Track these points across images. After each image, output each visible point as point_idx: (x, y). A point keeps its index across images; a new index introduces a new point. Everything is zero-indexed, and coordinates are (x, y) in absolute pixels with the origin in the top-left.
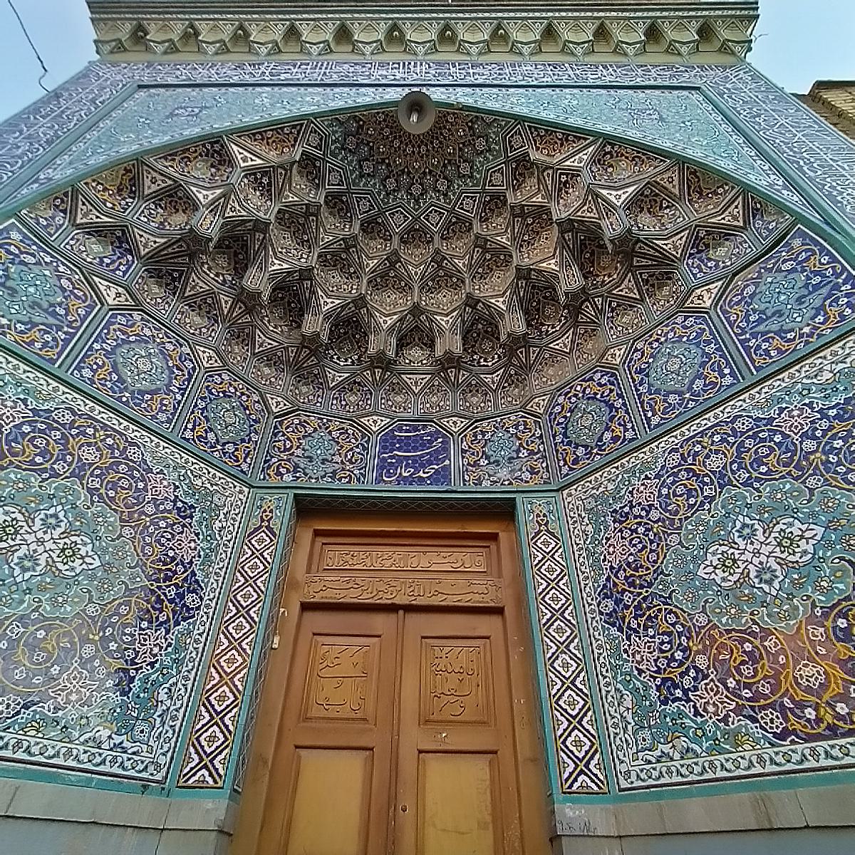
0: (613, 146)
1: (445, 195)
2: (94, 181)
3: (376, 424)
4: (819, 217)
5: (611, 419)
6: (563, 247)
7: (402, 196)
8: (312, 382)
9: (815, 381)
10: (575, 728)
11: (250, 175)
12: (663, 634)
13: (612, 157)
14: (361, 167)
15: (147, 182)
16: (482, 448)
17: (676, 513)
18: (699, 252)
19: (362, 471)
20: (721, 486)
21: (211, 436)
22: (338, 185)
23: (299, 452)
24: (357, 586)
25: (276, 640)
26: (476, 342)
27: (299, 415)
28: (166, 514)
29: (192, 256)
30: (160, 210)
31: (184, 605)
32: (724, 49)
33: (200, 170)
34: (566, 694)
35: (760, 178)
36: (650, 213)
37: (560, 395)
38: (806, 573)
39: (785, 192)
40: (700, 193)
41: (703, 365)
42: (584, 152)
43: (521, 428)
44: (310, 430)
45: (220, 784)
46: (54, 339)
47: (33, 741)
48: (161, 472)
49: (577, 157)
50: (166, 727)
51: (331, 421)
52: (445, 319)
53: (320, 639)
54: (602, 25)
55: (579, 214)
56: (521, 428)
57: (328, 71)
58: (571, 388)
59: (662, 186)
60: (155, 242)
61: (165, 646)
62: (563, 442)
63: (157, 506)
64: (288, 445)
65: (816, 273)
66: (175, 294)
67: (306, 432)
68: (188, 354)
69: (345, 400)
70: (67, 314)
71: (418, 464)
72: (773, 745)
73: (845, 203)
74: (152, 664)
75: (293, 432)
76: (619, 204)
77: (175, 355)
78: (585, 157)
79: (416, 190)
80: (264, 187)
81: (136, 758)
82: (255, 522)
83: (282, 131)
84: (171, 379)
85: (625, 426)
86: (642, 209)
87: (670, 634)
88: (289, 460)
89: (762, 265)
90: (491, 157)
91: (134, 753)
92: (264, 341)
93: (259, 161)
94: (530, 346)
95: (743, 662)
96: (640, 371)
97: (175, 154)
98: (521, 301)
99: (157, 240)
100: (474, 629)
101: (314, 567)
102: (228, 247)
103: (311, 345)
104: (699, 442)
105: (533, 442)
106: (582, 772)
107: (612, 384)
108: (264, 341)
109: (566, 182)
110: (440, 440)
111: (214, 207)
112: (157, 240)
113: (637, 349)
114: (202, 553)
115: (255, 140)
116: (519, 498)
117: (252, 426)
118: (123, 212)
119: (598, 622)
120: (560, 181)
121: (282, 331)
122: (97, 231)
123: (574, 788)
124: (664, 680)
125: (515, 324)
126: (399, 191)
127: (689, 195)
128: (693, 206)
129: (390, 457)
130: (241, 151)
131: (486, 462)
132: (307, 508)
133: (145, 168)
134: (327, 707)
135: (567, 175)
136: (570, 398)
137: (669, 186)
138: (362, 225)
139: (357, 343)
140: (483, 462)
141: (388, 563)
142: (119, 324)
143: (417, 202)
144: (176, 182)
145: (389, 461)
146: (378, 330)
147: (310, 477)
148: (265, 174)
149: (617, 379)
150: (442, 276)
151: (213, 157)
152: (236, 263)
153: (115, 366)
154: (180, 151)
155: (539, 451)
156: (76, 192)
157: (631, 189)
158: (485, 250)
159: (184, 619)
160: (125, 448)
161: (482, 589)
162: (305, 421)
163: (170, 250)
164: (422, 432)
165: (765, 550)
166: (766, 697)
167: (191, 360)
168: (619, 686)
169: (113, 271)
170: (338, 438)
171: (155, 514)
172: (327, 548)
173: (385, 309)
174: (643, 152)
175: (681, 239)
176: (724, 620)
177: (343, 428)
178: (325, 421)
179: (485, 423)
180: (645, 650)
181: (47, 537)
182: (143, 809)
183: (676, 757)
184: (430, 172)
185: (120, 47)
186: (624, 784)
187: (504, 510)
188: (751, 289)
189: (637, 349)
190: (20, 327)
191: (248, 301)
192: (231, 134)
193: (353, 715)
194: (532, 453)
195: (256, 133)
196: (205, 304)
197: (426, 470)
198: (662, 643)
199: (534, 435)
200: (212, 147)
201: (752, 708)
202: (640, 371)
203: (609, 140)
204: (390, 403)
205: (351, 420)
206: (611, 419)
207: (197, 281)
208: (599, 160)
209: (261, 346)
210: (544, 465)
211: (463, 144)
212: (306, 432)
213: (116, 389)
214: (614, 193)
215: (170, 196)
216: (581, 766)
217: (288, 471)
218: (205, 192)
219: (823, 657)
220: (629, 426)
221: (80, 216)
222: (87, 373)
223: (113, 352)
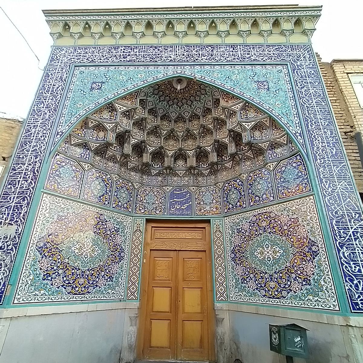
0: (249, 104)
1: (190, 106)
3: (169, 189)
4: (306, 152)
5: (240, 198)
6: (230, 137)
8: (147, 174)
9: (291, 208)
12: (244, 267)
13: (248, 107)
14: (160, 99)
15: (90, 123)
17: (252, 235)
18: (272, 149)
20: (264, 232)
21: (120, 203)
22: (152, 105)
26: (201, 158)
29: (107, 148)
30: (95, 131)
32: (304, 32)
33: (106, 115)
35: (293, 130)
36: (259, 130)
37: (227, 183)
38: (276, 261)
39: (299, 137)
40: (276, 126)
41: (267, 190)
42: (239, 105)
43: (214, 192)
44: (148, 192)
47: (97, 295)
48: (110, 221)
49: (236, 106)
50: (122, 287)
51: (154, 188)
53: (156, 259)
54: (255, 21)
55: (235, 128)
56: (214, 192)
57: (145, 54)
58: (230, 182)
60: (96, 145)
62: (226, 201)
65: (301, 172)
66: (103, 157)
68: (109, 178)
71: (182, 204)
72: (262, 297)
73: (315, 145)
74: (117, 273)
76: (248, 128)
77: (106, 180)
78: (239, 107)
79: (180, 104)
80: (127, 116)
82: (135, 228)
84: (106, 188)
85: (243, 202)
86: (256, 129)
87: (246, 267)
88: (142, 205)
89: (289, 161)
90: (207, 96)
92: (131, 165)
95: (260, 278)
96: (250, 185)
97: (97, 111)
98: (215, 148)
99: (96, 145)
103: (147, 165)
104: (261, 216)
105: (217, 198)
107: (242, 186)
108: (131, 165)
109: (232, 113)
110: (189, 194)
111: (113, 130)
112: (96, 145)
113: (250, 176)
115: (123, 100)
117: (130, 195)
118: (85, 137)
119: (230, 259)
120: (230, 113)
121: (136, 160)
122: (78, 145)
124: (243, 278)
125: (213, 158)
126: (174, 104)
127: (272, 126)
128: (272, 131)
129: (173, 201)
130: (119, 106)
132: (148, 221)
135: (233, 111)
136: (229, 186)
137: (266, 123)
138: (161, 117)
139: (161, 159)
140: (202, 203)
143: (180, 108)
144: (99, 122)
146: (168, 157)
147: (149, 210)
148: (127, 112)
149: (243, 184)
150: (189, 135)
151: (109, 108)
152: (120, 142)
153: (92, 191)
154: (99, 111)
155: (219, 201)
157: (253, 123)
158: (204, 128)
159: (122, 260)
162: (146, 189)
164: (183, 191)
165: (270, 252)
166: (263, 287)
167: (111, 180)
168: (233, 277)
169: (85, 158)
173: (170, 148)
174: (258, 110)
175: (267, 144)
176: (258, 267)
177: (157, 191)
178: (152, 188)
180: (240, 270)
182: (121, 305)
183: (243, 296)
184: (185, 98)
185: (60, 36)
186: (231, 299)
187: (208, 221)
188: (284, 168)
189: (250, 176)
190: (67, 189)
191: (126, 156)
193: (166, 279)
194: (217, 202)
195: (124, 98)
196: (113, 159)
198: (244, 269)
199: (218, 195)
201: (260, 289)
202: (250, 185)
203: (247, 102)
206: (240, 198)
207: (109, 152)
208: (244, 108)
209: (130, 166)
210: (220, 206)
211: (197, 91)
214: (247, 124)
218: (109, 125)
219: (276, 281)
220: (245, 203)
221: (72, 141)
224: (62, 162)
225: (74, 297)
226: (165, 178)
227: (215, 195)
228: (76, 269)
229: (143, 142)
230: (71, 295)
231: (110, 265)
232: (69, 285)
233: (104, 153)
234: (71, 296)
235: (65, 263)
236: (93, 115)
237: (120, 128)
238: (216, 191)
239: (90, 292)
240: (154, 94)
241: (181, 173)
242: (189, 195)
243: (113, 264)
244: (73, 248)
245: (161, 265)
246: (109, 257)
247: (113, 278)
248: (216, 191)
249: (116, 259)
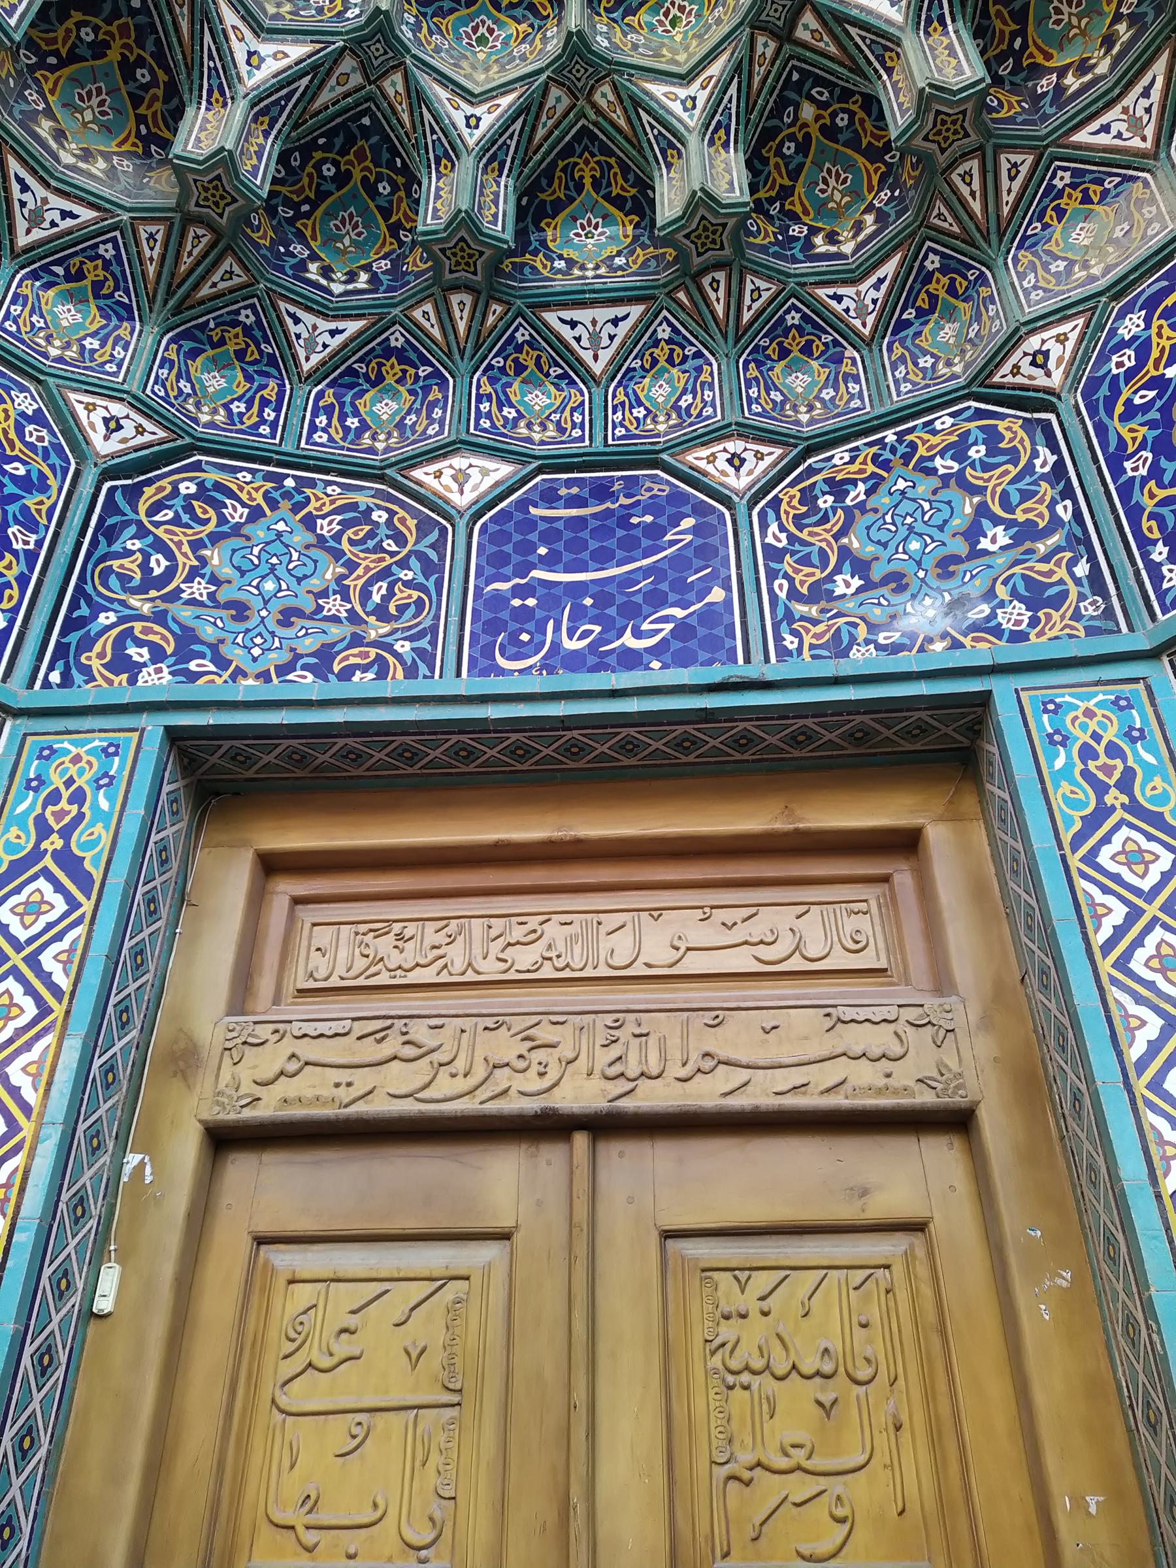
8: (240, 355)
16: (836, 537)
19: (424, 643)
23: (199, 589)
24: (410, 1051)
25: (109, 1279)
26: (794, 175)
27: (197, 466)
43: (977, 452)
44: (237, 514)
51: (312, 484)
52: (682, 93)
53: (284, 1259)
56: (977, 452)
64: (158, 564)
67: (222, 520)
69: (356, 413)
75: (176, 521)
88: (160, 618)
94: (998, 149)
100: (864, 1192)
101: (265, 985)
105: (1026, 495)
116: (1002, 689)
131: (857, 582)
134: (310, 1538)
145: (516, 602)
146: (449, 153)
155: (1056, 523)
161: (879, 1039)
162: (218, 486)
164: (623, 501)
170: (337, 537)
172: (308, 914)
178: (289, 483)
179: (840, 455)
194: (1026, 533)
197: (646, 626)
205: (381, 478)
209: (35, 220)
210: (1082, 569)
212: (222, 520)
217: (158, 654)
226: (435, 394)
227: (997, 481)
238: (992, 438)
241: (595, 338)
242: (695, 530)
245: (344, 1347)
248: (992, 438)
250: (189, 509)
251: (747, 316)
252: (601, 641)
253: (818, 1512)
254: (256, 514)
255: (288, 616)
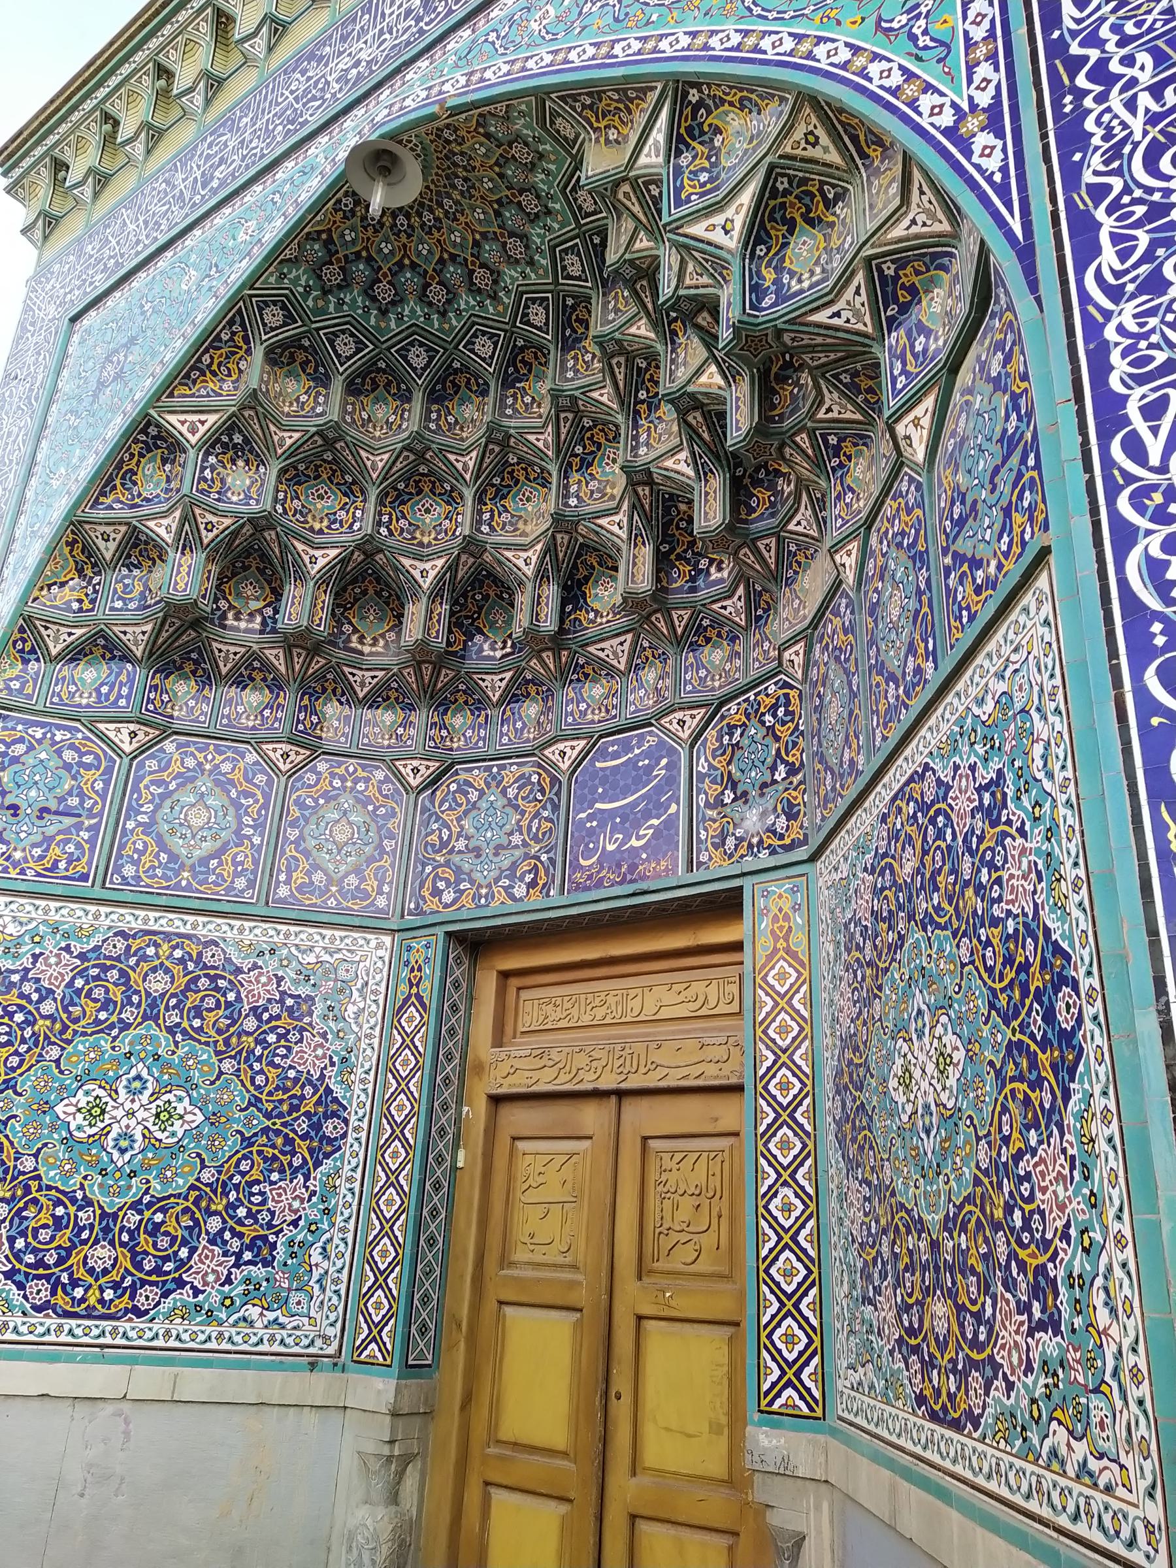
2: (42, 589)
7: (467, 303)
8: (466, 703)
10: (789, 1313)
11: (213, 446)
14: (374, 299)
15: (101, 543)
21: (318, 877)
22: (358, 351)
23: (461, 844)
25: (461, 1155)
28: (274, 1023)
30: (136, 572)
31: (324, 1136)
34: (782, 1258)
44: (474, 796)
45: (388, 1362)
46: (79, 846)
47: (181, 1329)
48: (255, 966)
50: (328, 1293)
53: (521, 1145)
59: (803, 160)
61: (306, 1196)
63: (259, 1019)
64: (445, 834)
67: (468, 801)
69: (521, 718)
70: (82, 803)
71: (629, 820)
74: (295, 1223)
75: (450, 808)
77: (238, 776)
80: (243, 450)
81: (298, 1333)
83: (220, 340)
88: (447, 864)
91: (295, 1328)
93: (212, 419)
100: (716, 1120)
101: (509, 1030)
102: (245, 568)
106: (789, 1383)
110: (664, 762)
111: (186, 544)
112: (144, 628)
114: (335, 1059)
115: (194, 382)
121: (386, 645)
122: (76, 654)
123: (775, 1407)
129: (590, 818)
133: (87, 527)
141: (600, 1013)
142: (151, 773)
147: (480, 886)
152: (269, 583)
156: (29, 620)
159: (327, 1156)
160: (200, 954)
161: (721, 1053)
163: (165, 635)
164: (637, 751)
170: (516, 798)
171: (259, 1027)
172: (524, 995)
177: (522, 776)
181: (136, 1106)
182: (318, 1387)
190: (37, 852)
192: (158, 400)
200: (147, 434)
204: (583, 706)
207: (224, 648)
208: (690, 130)
209: (363, 685)
212: (468, 801)
213: (170, 873)
215: (135, 546)
216: (790, 1374)
217: (449, 884)
222: (129, 870)
223: (153, 822)
224: (14, 742)
225: (60, 1326)
228: (74, 1201)
229: (368, 548)
230: (47, 1316)
231: (258, 1182)
232: (41, 1271)
233: (200, 654)
234: (48, 1322)
235: (24, 1173)
236: (96, 502)
237: (214, 519)
239: (147, 1312)
240: (330, 291)
241: (615, 653)
242: (667, 767)
243: (275, 1176)
244: (59, 1109)
245: (541, 1179)
246: (252, 1145)
247: (273, 1246)
249: (293, 1153)
250: (455, 799)
251: (679, 631)
252: (623, 843)
253: (690, 1245)
254: (482, 794)
255: (498, 849)
